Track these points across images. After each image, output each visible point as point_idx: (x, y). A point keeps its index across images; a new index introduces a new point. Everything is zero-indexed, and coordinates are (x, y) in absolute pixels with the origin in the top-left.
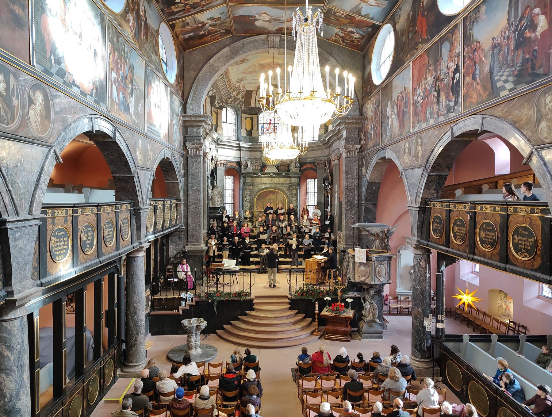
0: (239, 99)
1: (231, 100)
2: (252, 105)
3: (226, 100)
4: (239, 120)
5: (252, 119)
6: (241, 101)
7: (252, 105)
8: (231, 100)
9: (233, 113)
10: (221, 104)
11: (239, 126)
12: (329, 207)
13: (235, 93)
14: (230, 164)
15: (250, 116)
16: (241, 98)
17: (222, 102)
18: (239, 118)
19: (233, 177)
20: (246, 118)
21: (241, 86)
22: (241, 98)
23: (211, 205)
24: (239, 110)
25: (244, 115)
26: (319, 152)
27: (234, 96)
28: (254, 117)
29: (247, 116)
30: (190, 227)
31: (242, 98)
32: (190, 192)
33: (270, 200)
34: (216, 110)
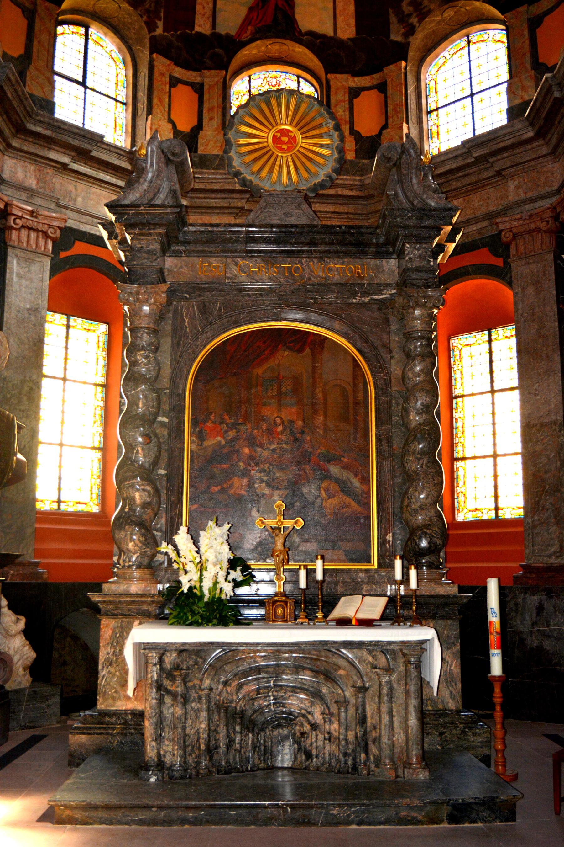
2: (202, 26)
4: (143, 82)
5: (199, 89)
7: (202, 26)
9: (118, 57)
11: (142, 105)
14: (80, 248)
15: (193, 76)
18: (144, 72)
19: (104, 328)
20: (174, 82)
24: (139, 41)
26: (512, 185)
28: (210, 78)
29: (178, 72)
33: (278, 379)
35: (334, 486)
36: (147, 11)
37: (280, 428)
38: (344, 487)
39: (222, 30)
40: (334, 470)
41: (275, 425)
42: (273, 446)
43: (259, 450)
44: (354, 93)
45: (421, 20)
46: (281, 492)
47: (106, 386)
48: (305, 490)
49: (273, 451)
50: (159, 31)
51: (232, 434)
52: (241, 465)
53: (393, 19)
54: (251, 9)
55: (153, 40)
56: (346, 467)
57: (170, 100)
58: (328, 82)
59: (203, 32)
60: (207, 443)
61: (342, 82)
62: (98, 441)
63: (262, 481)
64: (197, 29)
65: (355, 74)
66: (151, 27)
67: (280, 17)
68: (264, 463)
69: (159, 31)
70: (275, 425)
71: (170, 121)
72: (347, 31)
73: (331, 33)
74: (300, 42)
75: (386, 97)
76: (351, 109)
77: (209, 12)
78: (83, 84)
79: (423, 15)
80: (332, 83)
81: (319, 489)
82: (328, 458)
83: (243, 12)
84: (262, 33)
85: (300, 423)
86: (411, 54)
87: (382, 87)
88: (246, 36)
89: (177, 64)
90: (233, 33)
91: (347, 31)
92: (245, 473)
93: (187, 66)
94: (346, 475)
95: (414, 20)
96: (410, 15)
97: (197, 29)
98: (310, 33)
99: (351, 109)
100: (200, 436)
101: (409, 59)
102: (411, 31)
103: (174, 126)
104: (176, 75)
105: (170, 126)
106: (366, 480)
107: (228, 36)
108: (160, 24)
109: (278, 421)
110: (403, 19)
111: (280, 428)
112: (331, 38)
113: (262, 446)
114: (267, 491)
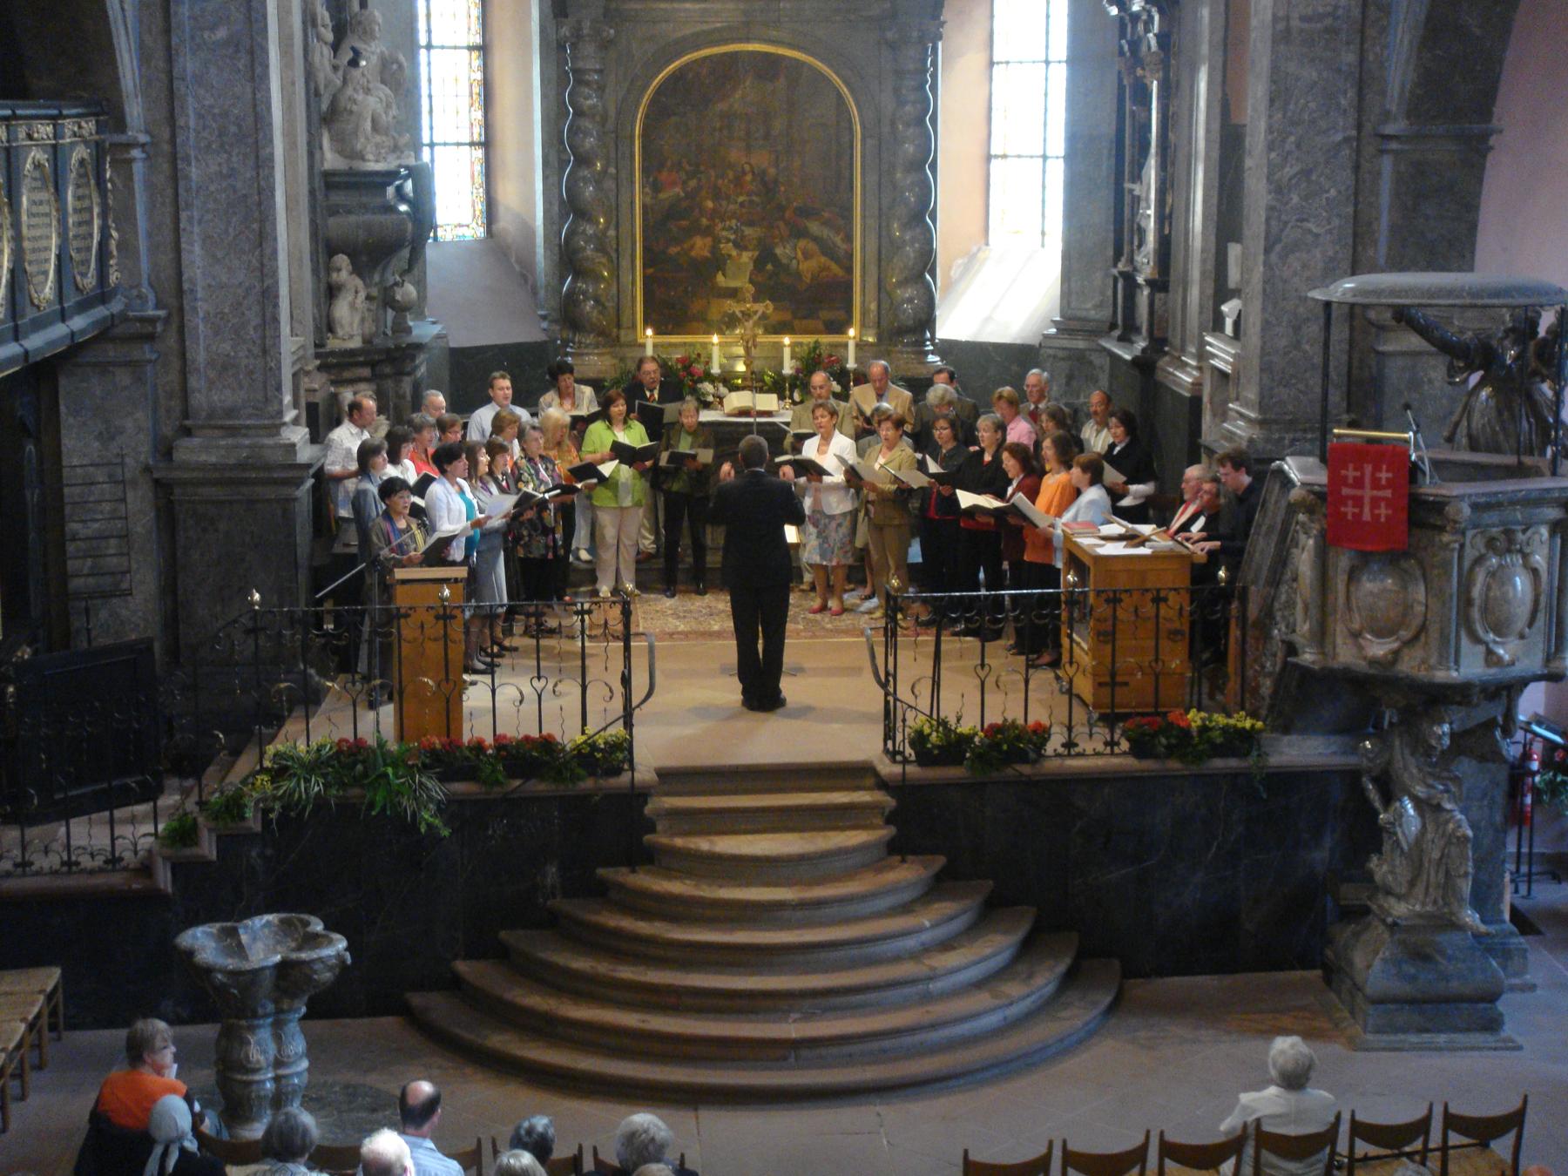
12: (1152, 163)
23: (331, 160)
30: (202, 307)
32: (188, 64)
35: (812, 246)
37: (749, 178)
38: (827, 250)
40: (814, 227)
41: (744, 173)
42: (741, 199)
43: (724, 203)
46: (750, 254)
47: (484, 49)
48: (778, 251)
49: (742, 205)
51: (693, 183)
52: (704, 221)
56: (826, 223)
60: (662, 196)
62: (478, 134)
63: (728, 240)
68: (730, 218)
70: (744, 173)
81: (795, 248)
82: (805, 212)
85: (772, 171)
92: (707, 232)
94: (826, 233)
100: (655, 187)
106: (849, 238)
109: (747, 168)
111: (749, 178)
113: (728, 198)
114: (734, 253)
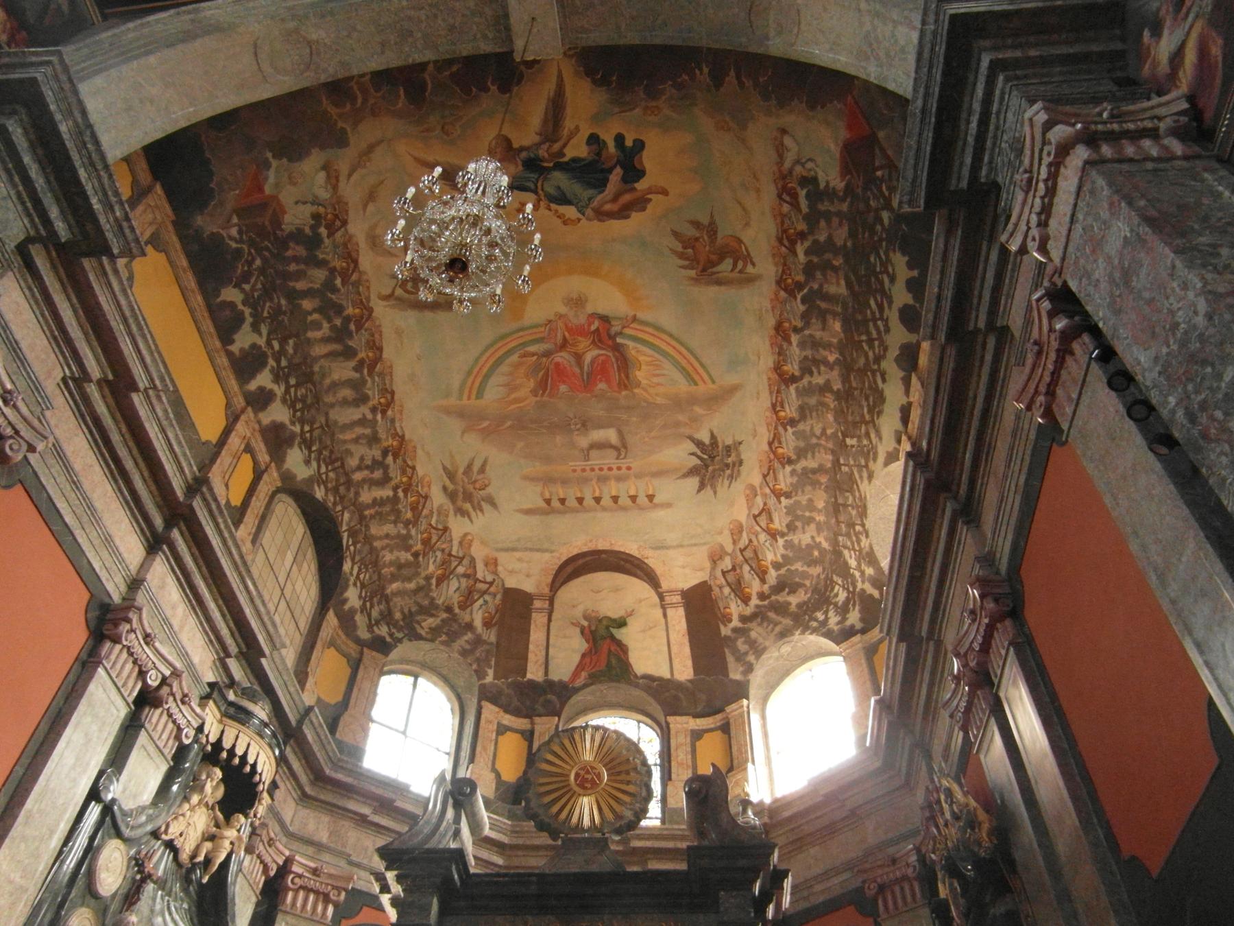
0: (469, 627)
1: (430, 622)
2: (534, 673)
3: (409, 618)
6: (478, 641)
7: (534, 673)
8: (430, 622)
10: (383, 631)
13: (451, 592)
15: (522, 723)
16: (478, 623)
17: (387, 617)
20: (502, 730)
21: (478, 552)
22: (478, 623)
25: (490, 710)
27: (449, 609)
29: (508, 720)
31: (487, 624)
34: (353, 649)
36: (478, 660)
39: (555, 676)
44: (697, 735)
45: (758, 657)
50: (489, 678)
53: (730, 659)
54: (584, 656)
55: (482, 687)
57: (496, 749)
58: (668, 724)
59: (536, 679)
61: (682, 725)
64: (529, 676)
65: (696, 716)
66: (480, 674)
67: (614, 661)
69: (489, 678)
71: (494, 770)
72: (684, 671)
73: (668, 676)
74: (637, 686)
75: (730, 738)
76: (694, 751)
77: (542, 660)
78: (404, 733)
79: (759, 652)
80: (671, 726)
83: (576, 659)
84: (594, 679)
86: (753, 692)
87: (725, 728)
88: (579, 682)
89: (506, 711)
90: (566, 679)
91: (684, 671)
93: (517, 713)
95: (751, 658)
96: (746, 653)
97: (529, 676)
98: (645, 677)
99: (694, 751)
101: (751, 697)
102: (749, 669)
103: (498, 775)
104: (505, 722)
105: (493, 776)
107: (560, 682)
108: (491, 672)
110: (740, 658)
112: (668, 680)
